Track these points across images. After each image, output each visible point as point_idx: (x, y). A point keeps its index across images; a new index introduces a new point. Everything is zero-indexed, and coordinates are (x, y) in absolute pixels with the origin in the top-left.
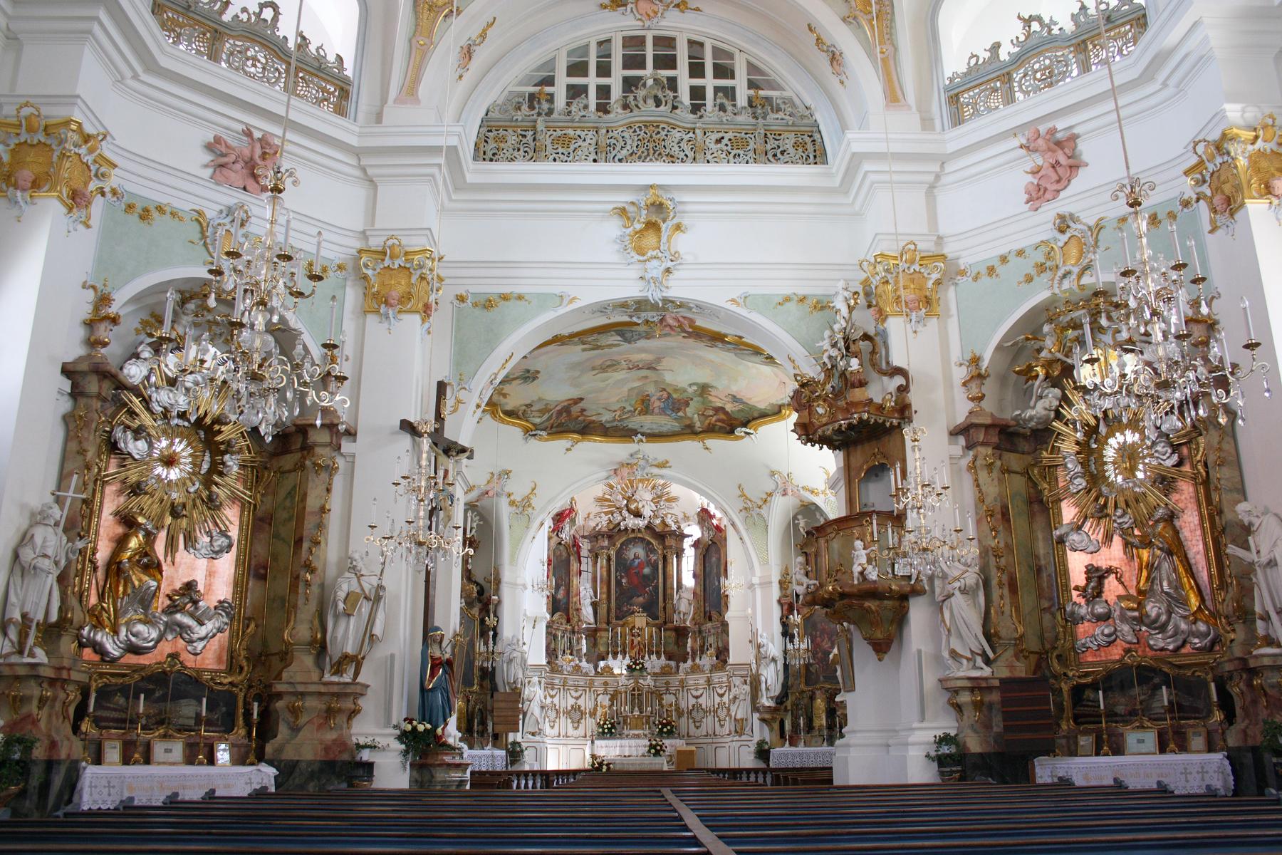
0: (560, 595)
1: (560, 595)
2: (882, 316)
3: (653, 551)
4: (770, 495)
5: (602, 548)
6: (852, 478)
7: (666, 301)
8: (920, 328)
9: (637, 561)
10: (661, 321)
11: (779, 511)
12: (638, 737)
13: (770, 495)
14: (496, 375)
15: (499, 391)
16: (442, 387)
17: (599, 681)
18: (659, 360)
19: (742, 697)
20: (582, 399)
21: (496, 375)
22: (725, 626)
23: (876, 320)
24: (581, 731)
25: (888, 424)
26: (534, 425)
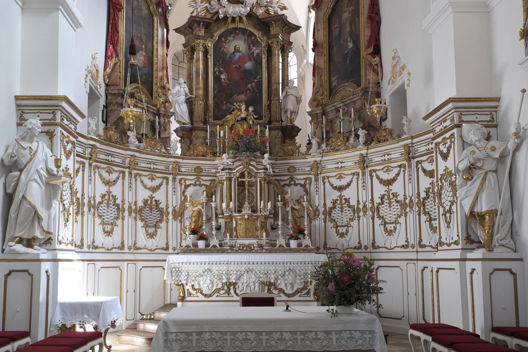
9: (238, 55)
12: (248, 249)
17: (189, 164)
24: (159, 240)
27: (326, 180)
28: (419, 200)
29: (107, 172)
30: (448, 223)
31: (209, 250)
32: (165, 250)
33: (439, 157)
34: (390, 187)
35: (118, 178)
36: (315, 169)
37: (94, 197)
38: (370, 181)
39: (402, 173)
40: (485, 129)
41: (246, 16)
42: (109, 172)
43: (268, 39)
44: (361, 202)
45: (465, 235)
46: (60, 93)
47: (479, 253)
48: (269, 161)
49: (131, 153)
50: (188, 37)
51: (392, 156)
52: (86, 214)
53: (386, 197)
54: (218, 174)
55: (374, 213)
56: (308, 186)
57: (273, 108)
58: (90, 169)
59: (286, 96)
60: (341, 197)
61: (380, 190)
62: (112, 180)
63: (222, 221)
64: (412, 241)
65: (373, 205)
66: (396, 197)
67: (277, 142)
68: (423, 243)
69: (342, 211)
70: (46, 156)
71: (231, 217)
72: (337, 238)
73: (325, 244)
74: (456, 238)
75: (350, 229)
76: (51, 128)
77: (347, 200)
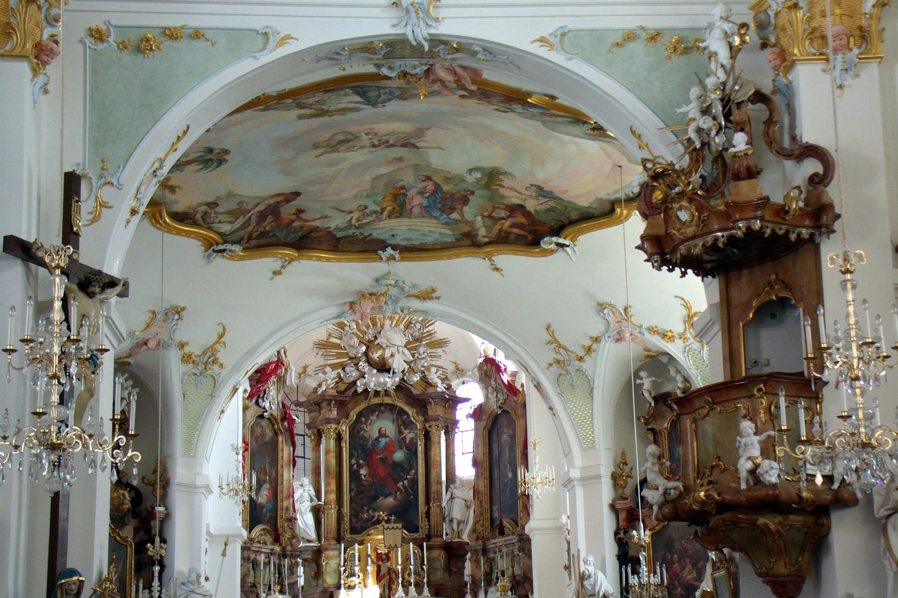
0: (263, 498)
1: (263, 498)
2: (785, 62)
4: (597, 340)
5: (328, 421)
6: (732, 321)
7: (435, 41)
8: (848, 81)
10: (428, 72)
11: (607, 367)
13: (597, 340)
14: (162, 161)
15: (166, 185)
16: (72, 184)
18: (420, 132)
20: (297, 194)
21: (162, 161)
22: (525, 543)
23: (776, 69)
25: (793, 237)
26: (221, 234)
43: (426, 421)
50: (313, 415)
57: (433, 518)
59: (452, 498)
67: (438, 566)
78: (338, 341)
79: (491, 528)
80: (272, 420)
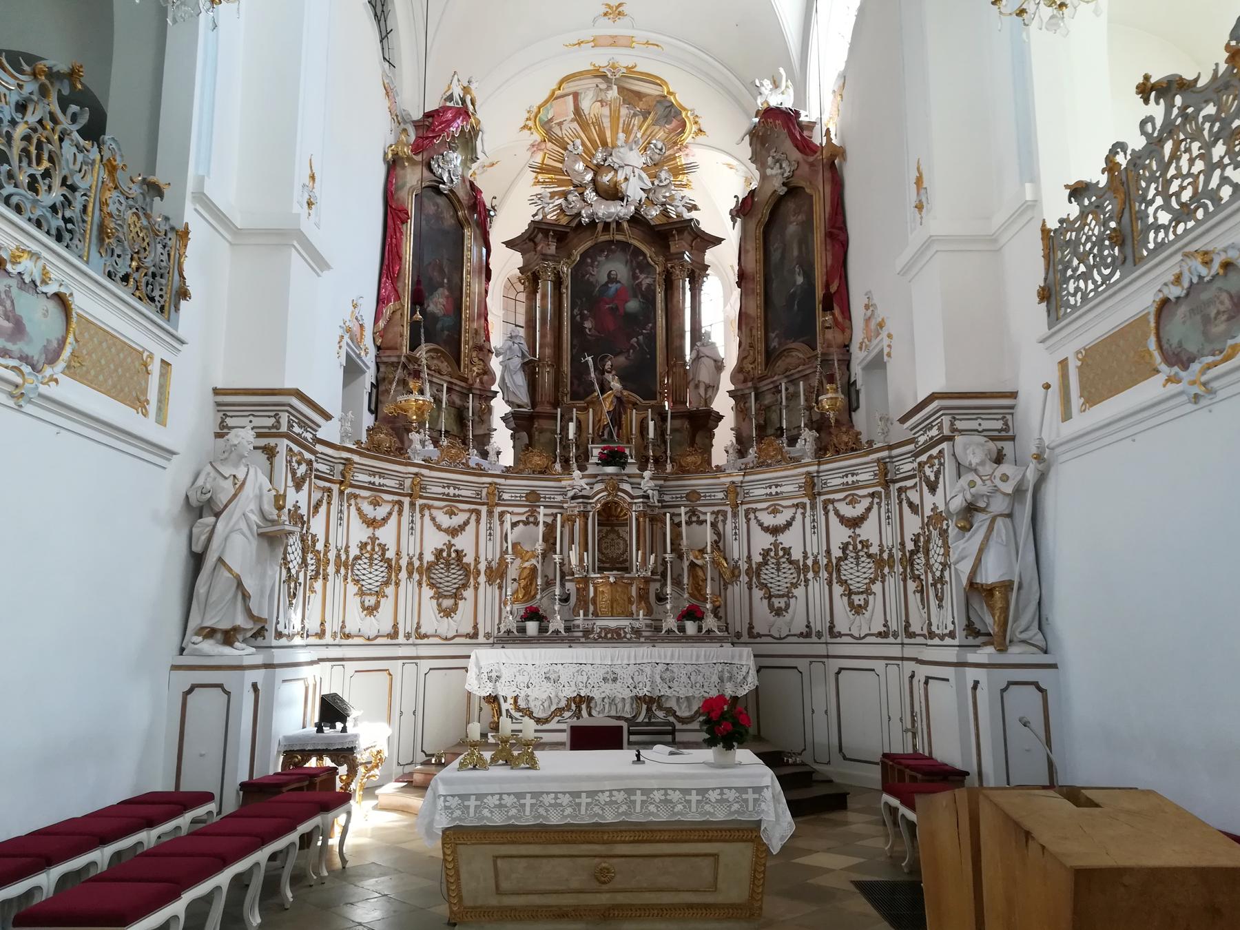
3: (645, 267)
9: (613, 287)
12: (614, 637)
17: (515, 488)
19: (999, 505)
24: (462, 620)
27: (752, 516)
28: (904, 554)
29: (371, 503)
30: (940, 599)
31: (546, 638)
32: (471, 638)
33: (925, 488)
34: (858, 531)
35: (390, 514)
36: (731, 496)
37: (347, 547)
38: (823, 518)
39: (875, 506)
40: (991, 445)
41: (628, 221)
42: (376, 503)
44: (809, 554)
45: (965, 622)
46: (288, 385)
47: (986, 654)
48: (652, 483)
49: (415, 470)
50: (527, 256)
51: (860, 478)
52: (331, 578)
53: (851, 547)
54: (565, 505)
55: (831, 574)
56: (720, 526)
58: (341, 500)
60: (776, 544)
61: (840, 534)
62: (379, 518)
63: (571, 586)
64: (893, 626)
65: (830, 561)
66: (868, 547)
68: (912, 629)
69: (778, 570)
70: (260, 489)
71: (586, 580)
72: (771, 617)
73: (751, 627)
74: (950, 627)
75: (792, 601)
76: (272, 442)
77: (787, 551)
78: (560, 165)
79: (766, 365)
80: (451, 197)
